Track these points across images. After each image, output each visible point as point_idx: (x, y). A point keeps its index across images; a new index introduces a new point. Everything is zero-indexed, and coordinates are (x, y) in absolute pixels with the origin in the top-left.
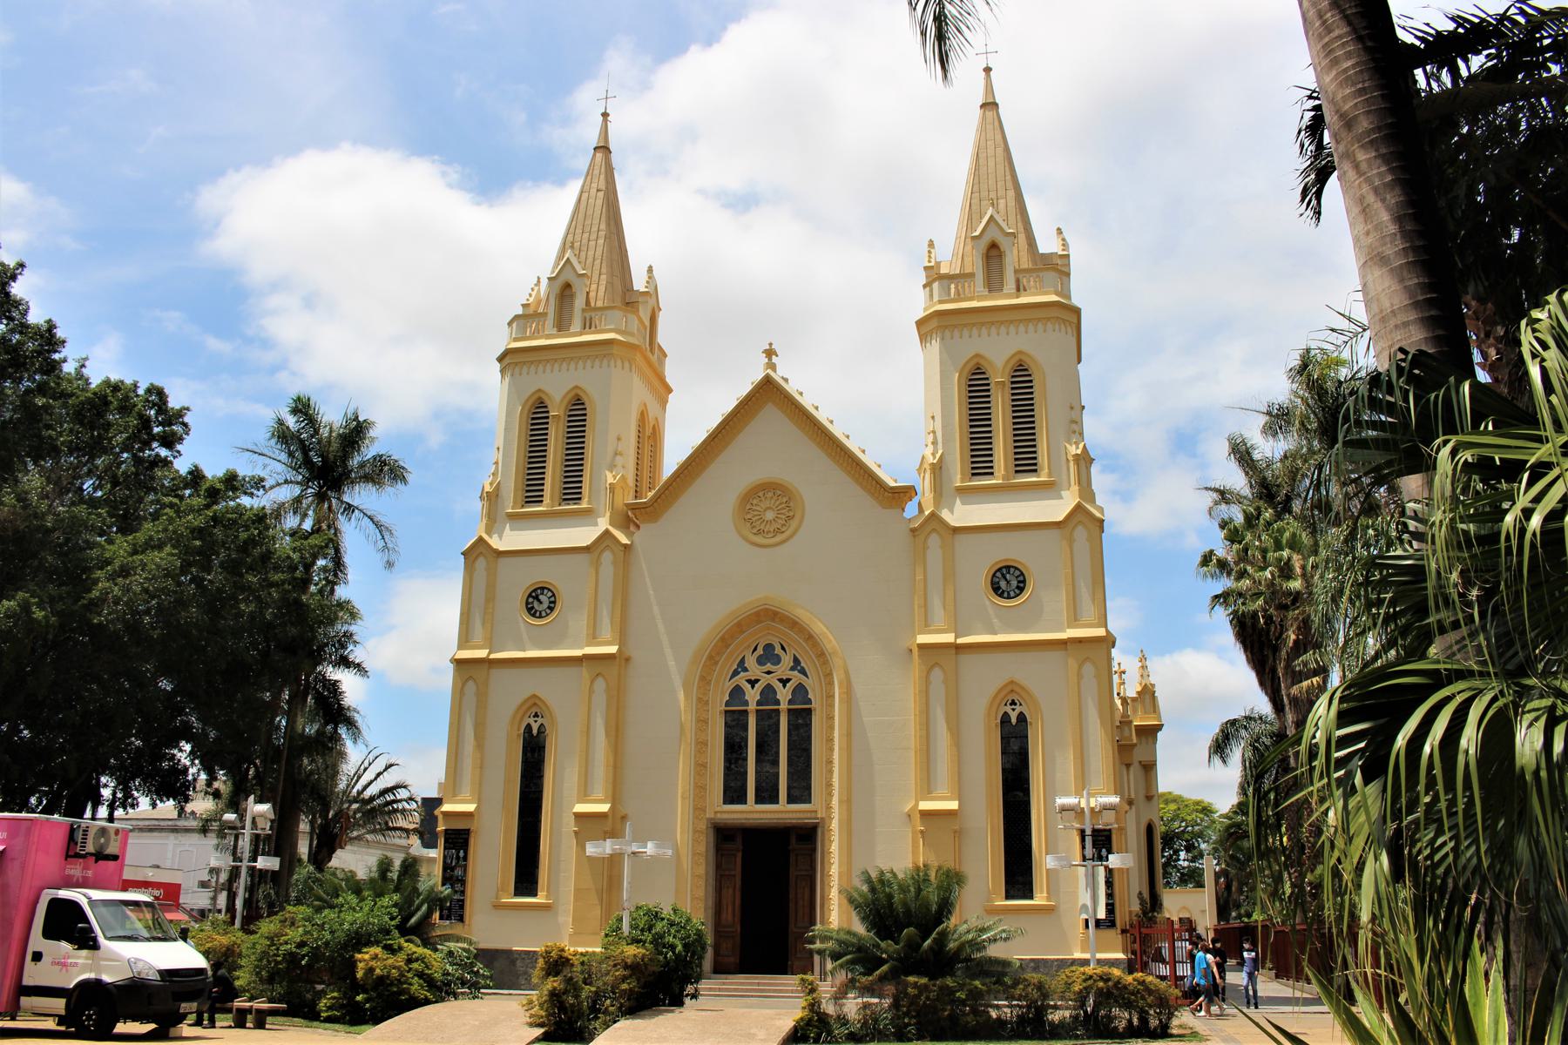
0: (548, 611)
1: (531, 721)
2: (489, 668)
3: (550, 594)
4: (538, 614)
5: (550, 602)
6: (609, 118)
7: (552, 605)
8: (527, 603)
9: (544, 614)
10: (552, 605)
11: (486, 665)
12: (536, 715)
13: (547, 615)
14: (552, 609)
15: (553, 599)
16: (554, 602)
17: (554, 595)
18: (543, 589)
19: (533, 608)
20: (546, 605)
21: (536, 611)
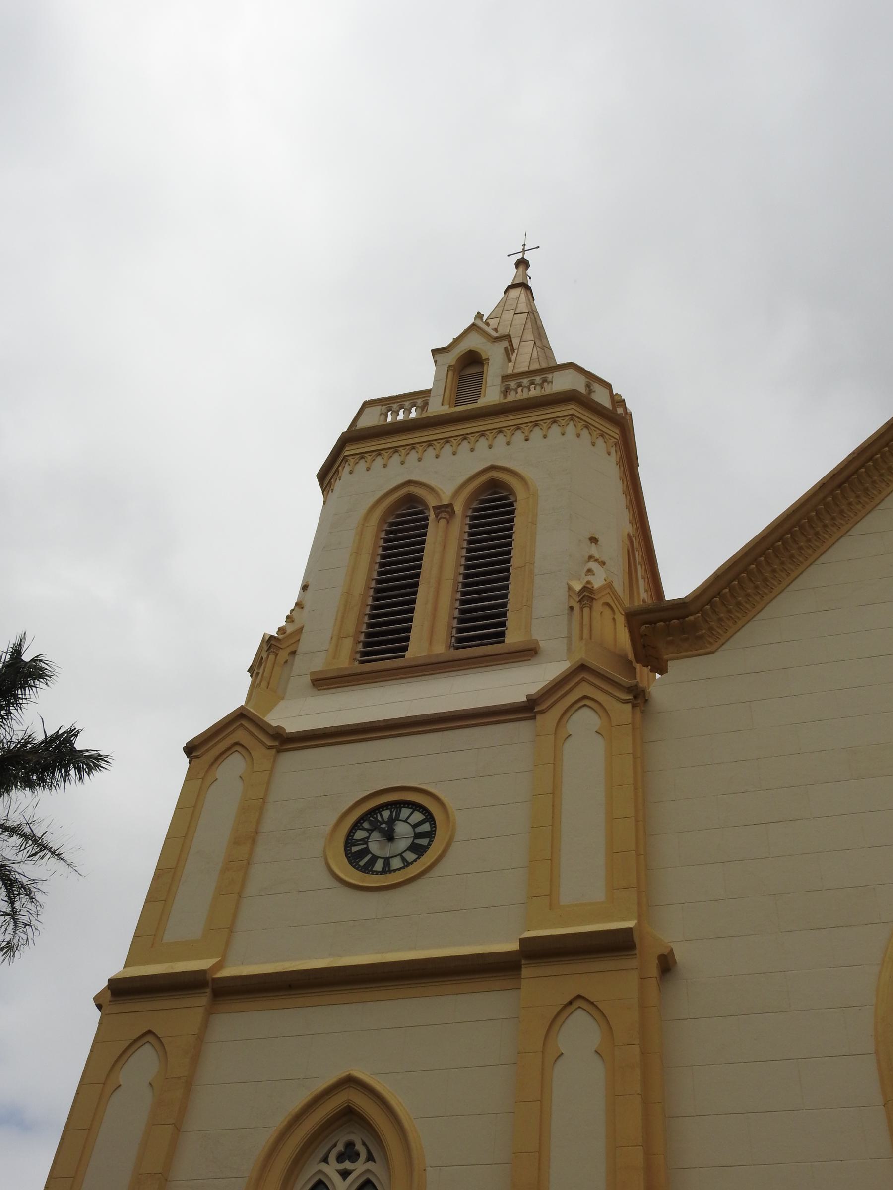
0: (410, 856)
1: (331, 1170)
2: (210, 1012)
3: (417, 817)
4: (379, 866)
5: (418, 836)
6: (529, 272)
7: (424, 842)
8: (349, 842)
9: (396, 863)
10: (424, 842)
11: (203, 1000)
12: (349, 1153)
13: (407, 864)
14: (418, 850)
15: (426, 827)
16: (430, 835)
17: (429, 817)
18: (398, 805)
19: (366, 851)
20: (402, 845)
21: (375, 858)
